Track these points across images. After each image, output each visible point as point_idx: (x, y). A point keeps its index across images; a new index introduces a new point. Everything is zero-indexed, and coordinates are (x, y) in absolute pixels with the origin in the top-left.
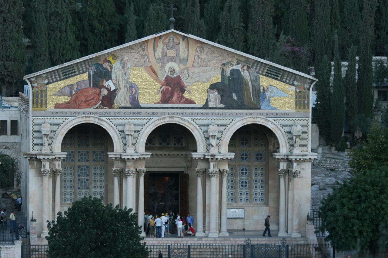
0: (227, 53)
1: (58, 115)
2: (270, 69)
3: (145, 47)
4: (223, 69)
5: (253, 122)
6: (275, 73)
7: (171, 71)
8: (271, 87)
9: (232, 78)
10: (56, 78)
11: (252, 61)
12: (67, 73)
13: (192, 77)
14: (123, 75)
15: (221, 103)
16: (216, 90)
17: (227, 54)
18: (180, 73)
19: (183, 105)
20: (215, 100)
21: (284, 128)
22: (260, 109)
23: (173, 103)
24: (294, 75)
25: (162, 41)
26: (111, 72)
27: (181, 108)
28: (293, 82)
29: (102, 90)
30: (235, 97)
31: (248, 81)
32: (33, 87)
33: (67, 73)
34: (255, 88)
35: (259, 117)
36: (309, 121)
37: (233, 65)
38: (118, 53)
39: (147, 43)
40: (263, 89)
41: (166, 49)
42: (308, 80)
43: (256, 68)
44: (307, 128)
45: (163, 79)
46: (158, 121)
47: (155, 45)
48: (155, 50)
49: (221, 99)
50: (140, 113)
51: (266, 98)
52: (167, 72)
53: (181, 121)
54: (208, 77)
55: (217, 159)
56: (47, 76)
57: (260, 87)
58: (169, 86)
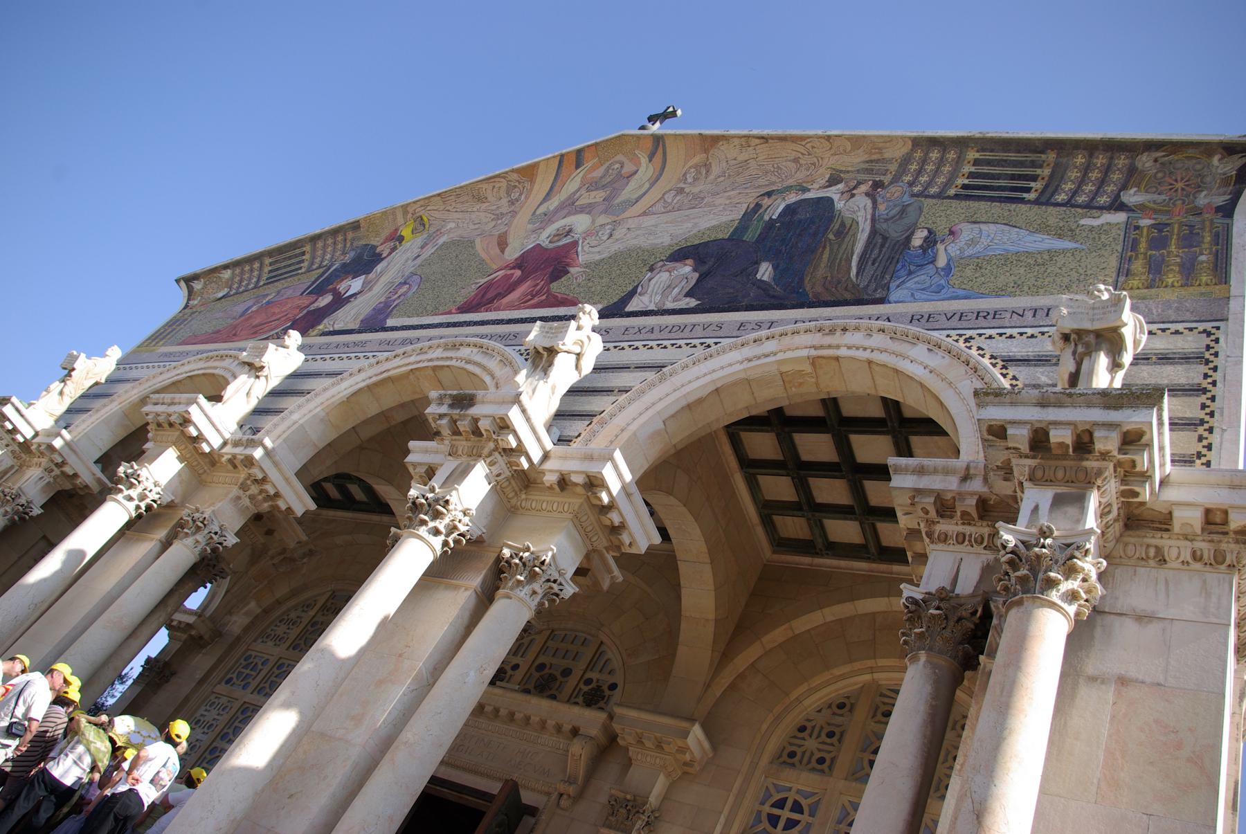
0: (794, 155)
1: (166, 359)
2: (986, 169)
3: (520, 195)
4: (758, 206)
5: (815, 348)
6: (1013, 177)
7: (558, 235)
8: (977, 226)
9: (783, 223)
10: (248, 285)
11: (899, 152)
12: (280, 272)
13: (617, 240)
14: (407, 261)
15: (689, 294)
16: (689, 262)
17: (796, 160)
18: (584, 235)
19: (527, 310)
20: (670, 287)
21: (1011, 371)
22: (882, 301)
23: (497, 309)
24: (1122, 161)
25: (581, 175)
26: (385, 258)
27: (509, 322)
28: (1118, 196)
29: (321, 298)
30: (765, 272)
31: (855, 222)
32: (186, 307)
33: (280, 272)
34: (885, 238)
35: (857, 329)
36: (1219, 334)
37: (809, 190)
38: (436, 214)
39: (532, 180)
40: (926, 239)
41: (583, 191)
42: (1215, 160)
43: (917, 178)
44: (1203, 369)
45: (517, 255)
46: (398, 359)
47: (556, 188)
48: (545, 199)
49: (698, 281)
50: (363, 344)
51: (933, 261)
52: (544, 239)
53: (479, 358)
54: (681, 231)
55: (476, 420)
56: (232, 279)
57: (912, 233)
58: (520, 268)
